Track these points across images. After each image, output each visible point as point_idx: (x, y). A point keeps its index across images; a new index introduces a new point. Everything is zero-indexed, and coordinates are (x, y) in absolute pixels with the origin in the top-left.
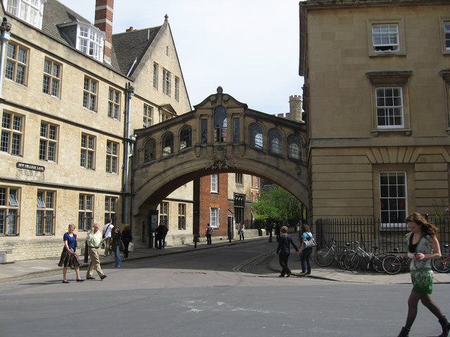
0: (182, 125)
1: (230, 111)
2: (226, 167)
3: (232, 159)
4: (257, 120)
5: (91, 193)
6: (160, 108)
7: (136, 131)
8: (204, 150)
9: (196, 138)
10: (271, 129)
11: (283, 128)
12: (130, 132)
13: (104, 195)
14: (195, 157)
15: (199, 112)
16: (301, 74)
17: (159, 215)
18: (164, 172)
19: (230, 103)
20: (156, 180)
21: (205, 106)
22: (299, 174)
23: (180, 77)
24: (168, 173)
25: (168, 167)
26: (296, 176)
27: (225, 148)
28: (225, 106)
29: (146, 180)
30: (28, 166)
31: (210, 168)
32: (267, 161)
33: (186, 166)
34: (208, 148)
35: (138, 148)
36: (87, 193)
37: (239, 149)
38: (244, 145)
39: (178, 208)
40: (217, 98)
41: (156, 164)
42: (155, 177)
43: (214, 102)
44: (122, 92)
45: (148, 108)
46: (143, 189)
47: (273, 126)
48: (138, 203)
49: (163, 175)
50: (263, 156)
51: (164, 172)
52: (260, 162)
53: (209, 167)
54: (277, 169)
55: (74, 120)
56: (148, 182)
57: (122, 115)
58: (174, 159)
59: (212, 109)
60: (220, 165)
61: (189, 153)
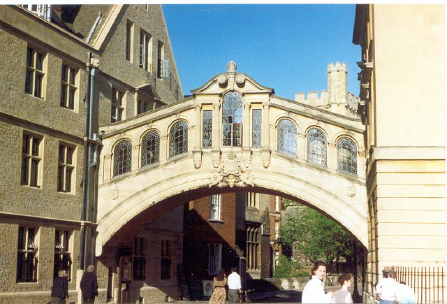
1: (248, 99)
2: (241, 184)
9: (194, 138)
16: (355, 41)
17: (133, 256)
18: (145, 190)
20: (133, 202)
24: (150, 192)
27: (238, 155)
29: (115, 203)
46: (111, 216)
49: (144, 195)
59: (221, 95)
60: (231, 182)
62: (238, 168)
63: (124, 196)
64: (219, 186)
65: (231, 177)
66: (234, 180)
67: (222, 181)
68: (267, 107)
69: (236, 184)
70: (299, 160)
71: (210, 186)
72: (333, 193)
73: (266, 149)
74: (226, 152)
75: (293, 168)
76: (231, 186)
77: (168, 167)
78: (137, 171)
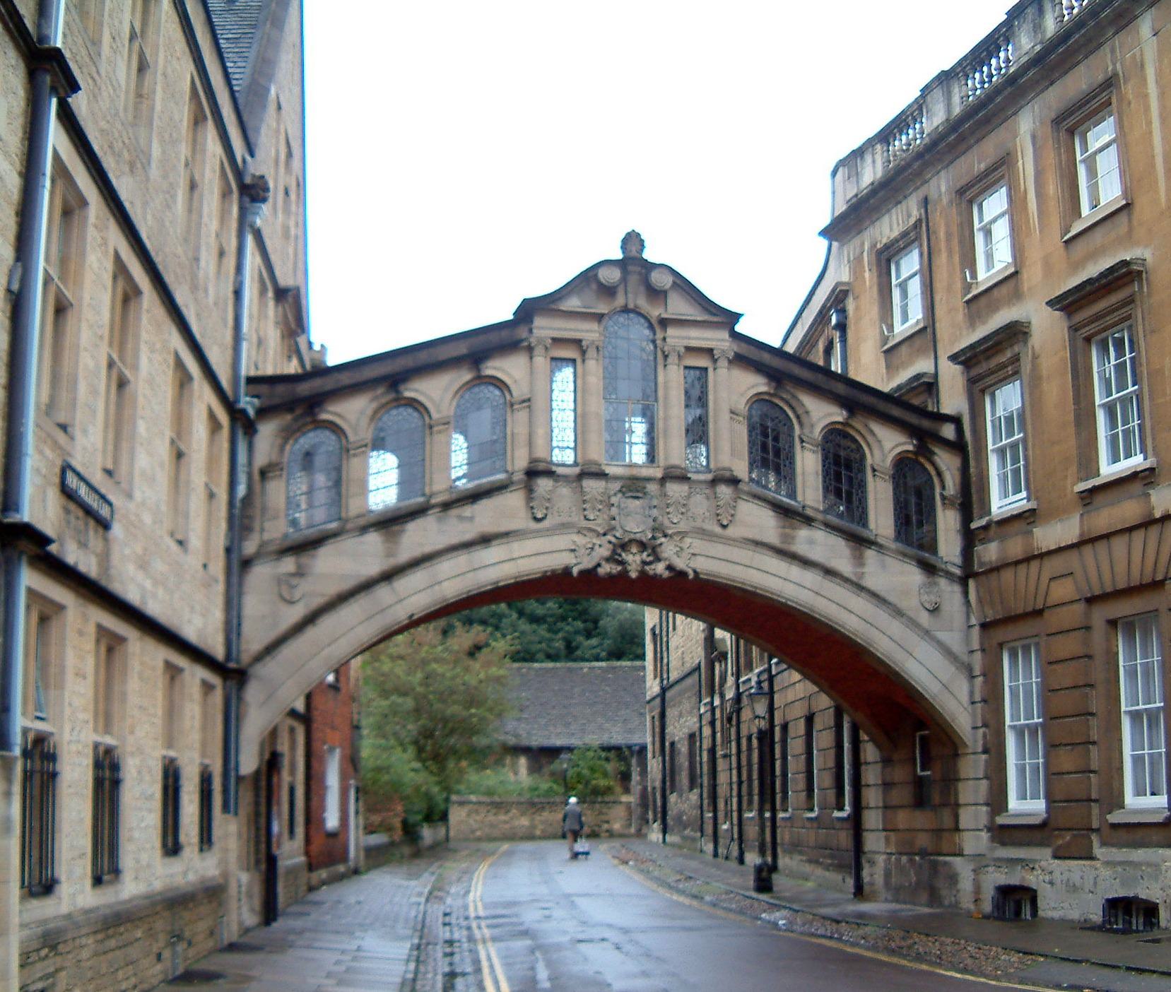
0: (466, 376)
1: (676, 337)
2: (660, 568)
3: (683, 535)
7: (251, 381)
8: (565, 491)
14: (521, 520)
15: (544, 327)
18: (388, 576)
19: (678, 306)
22: (935, 610)
23: (301, 179)
25: (404, 556)
26: (924, 618)
27: (652, 488)
30: (83, 491)
32: (815, 554)
37: (708, 498)
38: (734, 482)
41: (348, 544)
42: (344, 598)
43: (608, 291)
47: (837, 415)
49: (383, 593)
51: (388, 576)
53: (587, 564)
54: (860, 588)
56: (311, 619)
57: (231, 296)
59: (599, 317)
60: (634, 560)
63: (323, 595)
64: (601, 571)
66: (638, 558)
67: (608, 560)
68: (726, 363)
69: (647, 568)
70: (809, 512)
71: (575, 571)
72: (891, 598)
73: (727, 474)
74: (616, 478)
76: (634, 575)
77: (454, 512)
78: (362, 522)
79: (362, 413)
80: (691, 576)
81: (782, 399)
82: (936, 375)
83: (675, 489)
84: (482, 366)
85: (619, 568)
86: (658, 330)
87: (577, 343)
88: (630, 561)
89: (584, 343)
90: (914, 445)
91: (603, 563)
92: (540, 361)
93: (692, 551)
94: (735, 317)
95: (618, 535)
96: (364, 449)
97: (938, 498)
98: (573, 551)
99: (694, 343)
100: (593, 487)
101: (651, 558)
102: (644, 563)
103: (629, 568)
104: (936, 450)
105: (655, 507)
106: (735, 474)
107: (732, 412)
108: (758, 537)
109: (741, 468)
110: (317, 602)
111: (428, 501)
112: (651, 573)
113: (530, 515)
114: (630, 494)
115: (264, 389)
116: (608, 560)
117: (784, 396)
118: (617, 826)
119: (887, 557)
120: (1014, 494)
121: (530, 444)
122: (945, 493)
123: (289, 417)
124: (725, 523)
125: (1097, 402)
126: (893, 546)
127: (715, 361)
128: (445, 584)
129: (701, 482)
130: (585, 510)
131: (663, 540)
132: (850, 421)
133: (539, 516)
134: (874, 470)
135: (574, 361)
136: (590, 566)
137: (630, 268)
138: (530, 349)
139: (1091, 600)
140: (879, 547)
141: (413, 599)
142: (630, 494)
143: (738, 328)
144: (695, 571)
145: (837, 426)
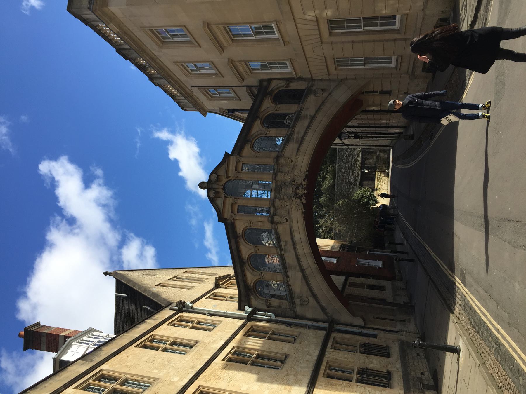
1: (232, 173)
2: (304, 183)
4: (248, 141)
5: (324, 363)
6: (217, 286)
8: (278, 212)
10: (262, 124)
11: (263, 108)
12: (242, 313)
13: (328, 349)
14: (287, 226)
15: (227, 215)
18: (302, 270)
21: (221, 207)
22: (323, 91)
24: (305, 264)
25: (295, 263)
26: (325, 95)
27: (278, 184)
28: (224, 180)
31: (305, 206)
32: (302, 131)
33: (297, 236)
34: (277, 205)
35: (265, 307)
36: (323, 368)
37: (283, 166)
38: (278, 158)
39: (355, 288)
40: (214, 189)
41: (291, 281)
43: (217, 194)
44: (180, 314)
45: (211, 295)
46: (324, 305)
47: (258, 122)
48: (345, 316)
49: (308, 272)
50: (295, 135)
51: (302, 270)
52: (303, 139)
53: (302, 206)
54: (313, 118)
55: (199, 367)
57: (213, 318)
58: (286, 255)
59: (225, 197)
60: (301, 191)
61: (280, 232)
62: (290, 185)
63: (307, 291)
65: (298, 191)
66: (301, 190)
67: (301, 200)
68: (241, 159)
69: (304, 188)
70: (289, 133)
71: (304, 210)
73: (275, 160)
75: (295, 140)
76: (306, 192)
77: (283, 247)
78: (285, 277)
79: (251, 273)
80: (307, 173)
81: (253, 140)
82: (247, 86)
83: (280, 177)
84: (239, 235)
85: (304, 196)
86: (230, 178)
87: (232, 205)
88: (302, 192)
89: (233, 203)
90: (269, 96)
91: (302, 201)
92: (237, 217)
93: (299, 173)
94: (226, 153)
95: (293, 196)
96: (262, 274)
97: (286, 89)
98: (297, 210)
99: (234, 168)
100: (278, 203)
101: (301, 186)
102: (302, 188)
103: (304, 193)
104: (271, 89)
105: (285, 184)
106: (275, 157)
107: (256, 157)
108: (296, 150)
109: (274, 155)
110: (309, 292)
111: (280, 255)
112: (306, 186)
113: (286, 223)
114: (280, 191)
115: (242, 304)
116: (301, 200)
117: (252, 139)
118: (386, 156)
119: (305, 108)
120: (287, 65)
121: (264, 222)
122: (285, 86)
123: (252, 297)
124: (291, 161)
125: (254, 38)
126: (301, 105)
127: (240, 161)
128: (305, 252)
129: (277, 169)
130: (284, 206)
131: (295, 182)
132: (261, 118)
133: (286, 221)
134: (277, 110)
135: (238, 206)
136: (302, 205)
137: (210, 186)
138: (234, 220)
139: (322, 42)
140: (301, 110)
141: (309, 263)
142: (280, 191)
143: (230, 152)
144: (306, 171)
145: (262, 121)
